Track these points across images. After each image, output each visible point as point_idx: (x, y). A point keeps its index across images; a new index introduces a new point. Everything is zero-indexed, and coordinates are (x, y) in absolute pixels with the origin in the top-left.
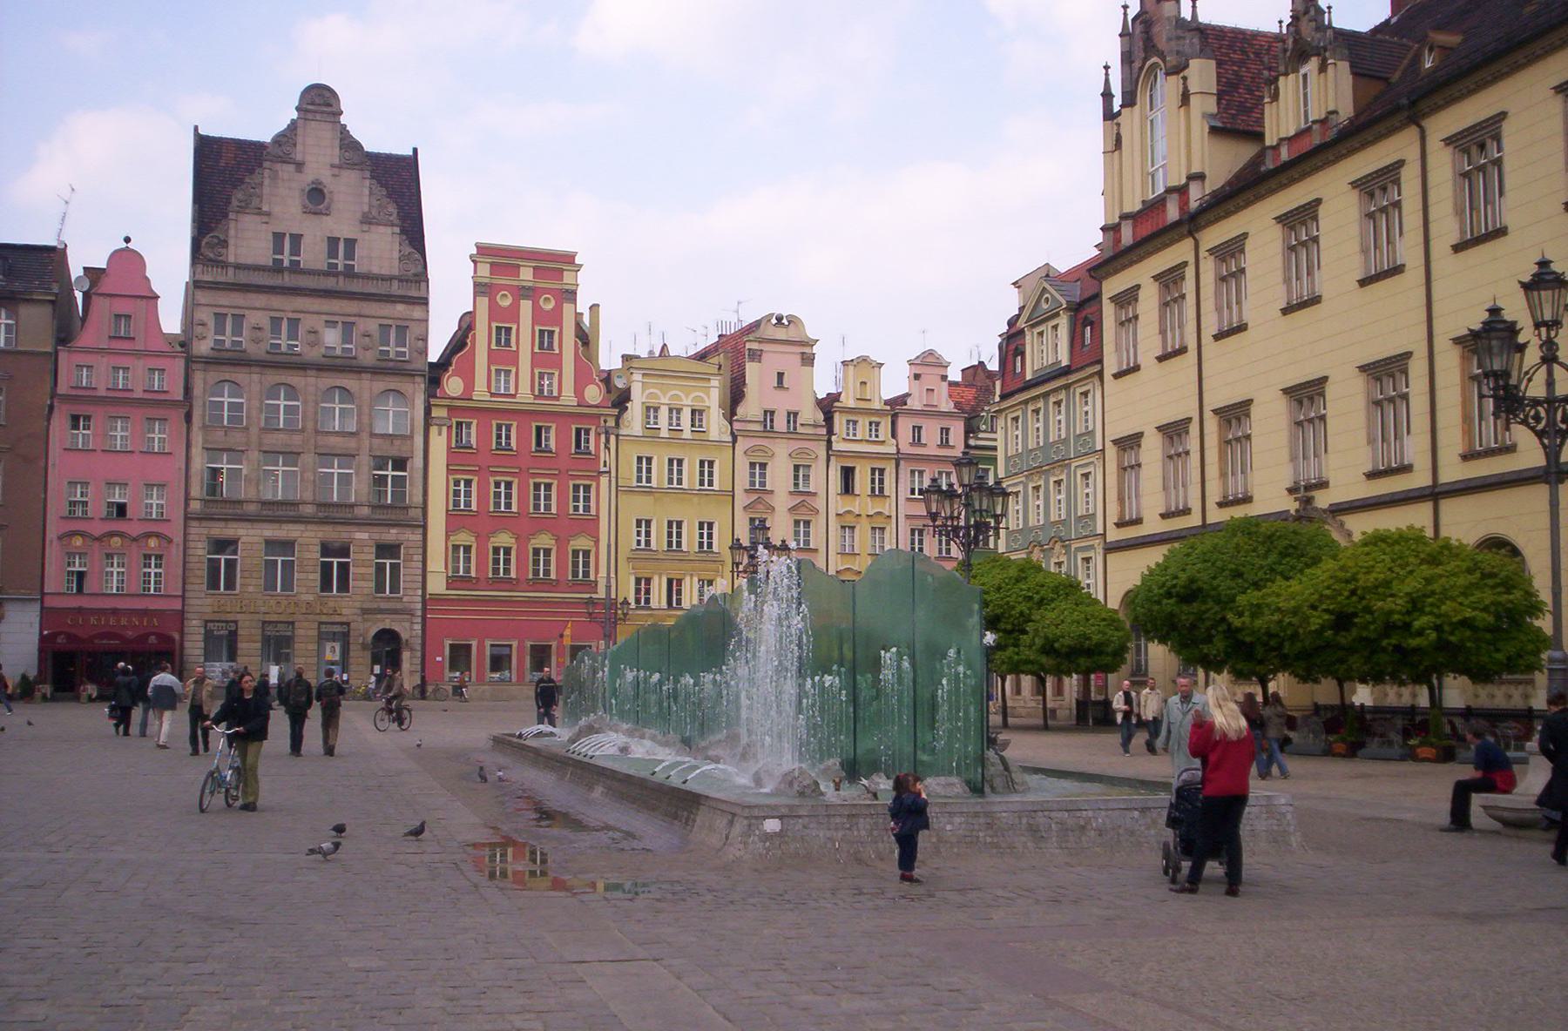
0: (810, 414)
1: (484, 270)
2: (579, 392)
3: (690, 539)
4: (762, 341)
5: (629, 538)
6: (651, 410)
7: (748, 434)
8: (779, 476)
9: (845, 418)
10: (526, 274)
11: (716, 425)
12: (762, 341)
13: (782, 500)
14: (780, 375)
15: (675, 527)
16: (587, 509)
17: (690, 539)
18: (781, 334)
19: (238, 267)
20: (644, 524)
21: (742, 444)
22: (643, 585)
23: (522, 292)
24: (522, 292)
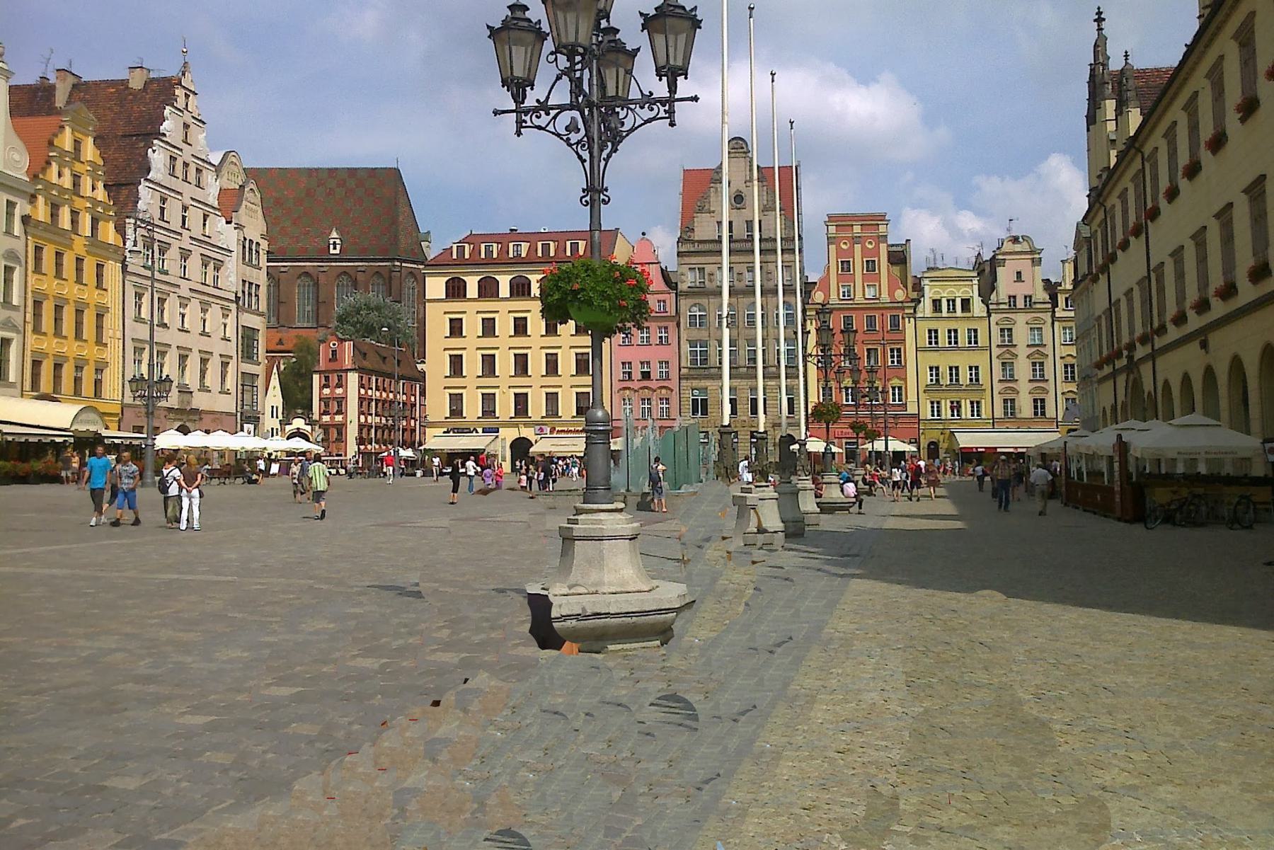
0: (1041, 295)
1: (832, 229)
2: (891, 293)
3: (965, 377)
4: (1004, 254)
5: (927, 378)
6: (936, 304)
7: (998, 311)
8: (1022, 336)
9: (1064, 296)
10: (857, 229)
11: (978, 308)
12: (1004, 254)
13: (1022, 351)
14: (1019, 274)
15: (954, 370)
16: (899, 362)
17: (965, 377)
18: (1018, 248)
19: (700, 242)
20: (935, 369)
21: (994, 318)
22: (936, 406)
23: (855, 240)
24: (855, 240)
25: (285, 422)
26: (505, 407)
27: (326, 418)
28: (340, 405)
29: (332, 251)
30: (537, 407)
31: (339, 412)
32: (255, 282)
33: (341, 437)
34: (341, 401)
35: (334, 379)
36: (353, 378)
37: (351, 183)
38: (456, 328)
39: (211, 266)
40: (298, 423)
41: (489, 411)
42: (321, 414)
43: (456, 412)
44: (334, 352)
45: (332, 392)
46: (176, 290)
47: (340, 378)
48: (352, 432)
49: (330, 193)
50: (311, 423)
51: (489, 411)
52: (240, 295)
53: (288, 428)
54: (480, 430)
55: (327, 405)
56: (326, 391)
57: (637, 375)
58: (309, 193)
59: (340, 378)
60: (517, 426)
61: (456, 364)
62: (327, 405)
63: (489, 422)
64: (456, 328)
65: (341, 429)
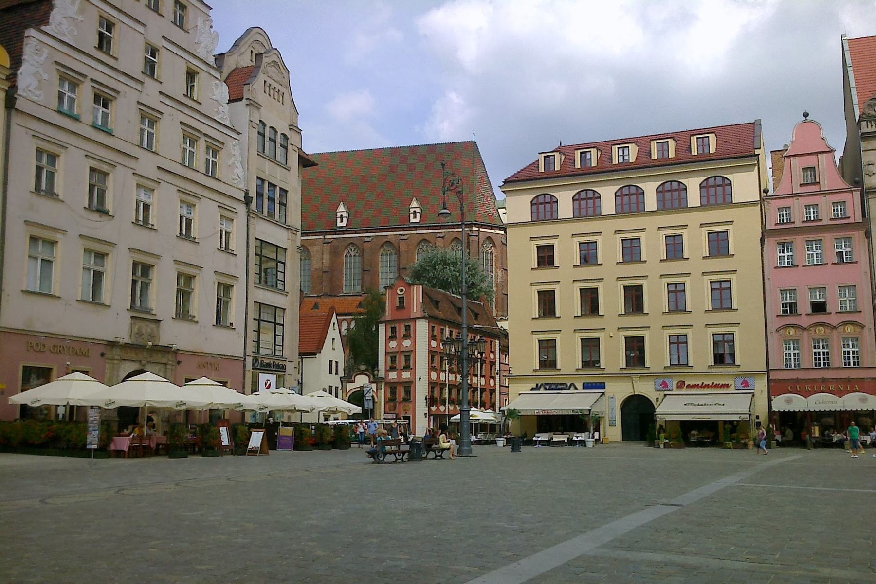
25: (348, 378)
26: (613, 355)
27: (393, 376)
28: (408, 359)
29: (412, 220)
30: (657, 355)
31: (407, 367)
32: (280, 185)
33: (409, 397)
34: (409, 357)
35: (401, 330)
36: (422, 328)
37: (430, 158)
38: (546, 257)
39: (202, 143)
40: (362, 380)
41: (591, 361)
42: (386, 371)
43: (548, 363)
44: (401, 300)
45: (400, 344)
46: (132, 164)
47: (408, 328)
48: (421, 391)
49: (411, 168)
50: (376, 380)
51: (591, 361)
52: (253, 194)
53: (350, 386)
54: (579, 386)
55: (393, 359)
56: (393, 344)
57: (804, 307)
58: (392, 169)
59: (408, 328)
60: (629, 377)
61: (547, 303)
62: (393, 359)
63: (591, 375)
64: (546, 257)
65: (408, 387)
